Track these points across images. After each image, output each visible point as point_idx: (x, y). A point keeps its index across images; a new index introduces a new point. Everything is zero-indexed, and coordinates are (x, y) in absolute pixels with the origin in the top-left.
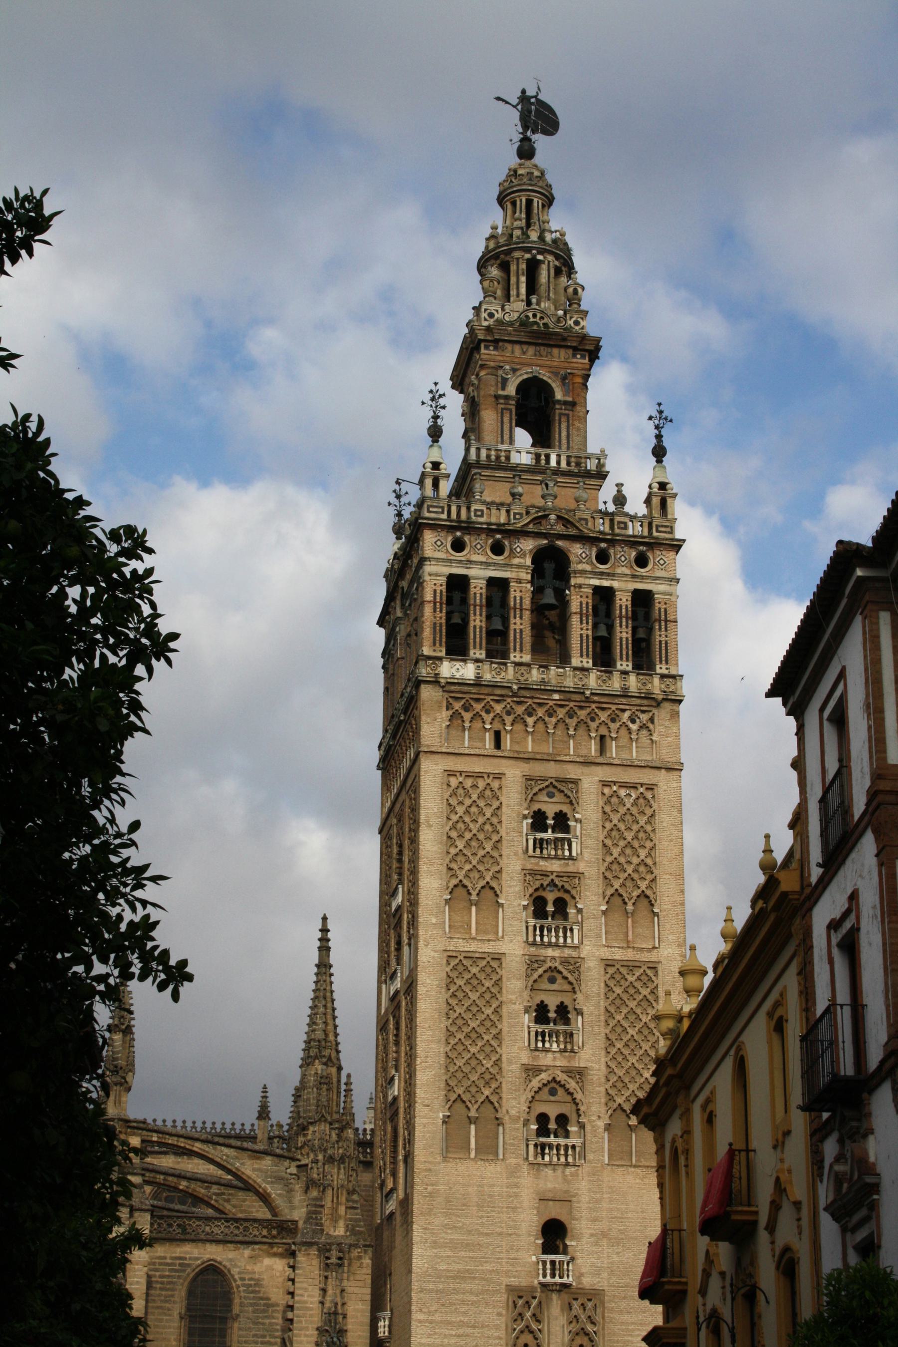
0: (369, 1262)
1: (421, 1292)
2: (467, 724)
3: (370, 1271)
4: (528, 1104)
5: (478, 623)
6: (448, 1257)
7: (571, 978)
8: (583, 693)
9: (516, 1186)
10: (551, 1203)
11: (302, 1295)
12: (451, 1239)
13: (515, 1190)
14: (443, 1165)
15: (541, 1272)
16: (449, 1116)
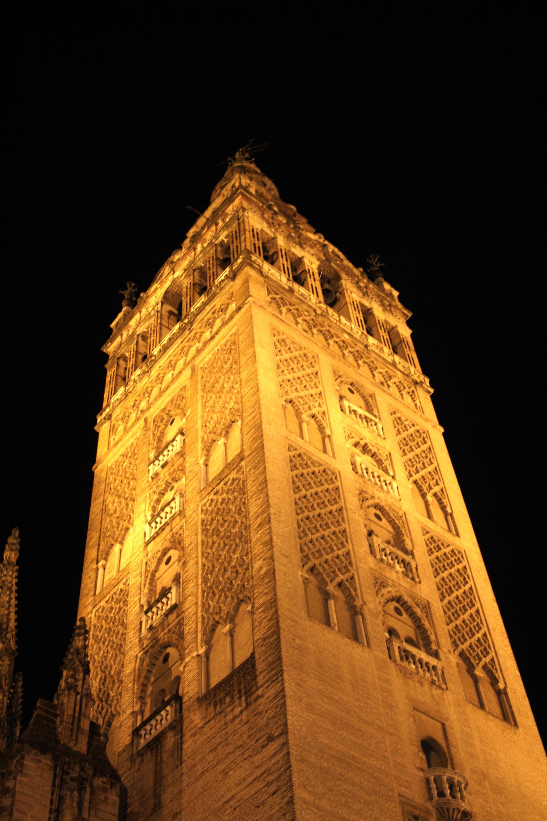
0: (117, 799)
1: (303, 761)
2: (284, 310)
3: (116, 812)
4: (381, 606)
5: (285, 262)
6: (329, 730)
7: (396, 521)
8: (366, 346)
9: (387, 681)
10: (424, 717)
11: (23, 813)
12: (327, 709)
13: (387, 686)
14: (308, 623)
15: (435, 792)
16: (306, 579)
